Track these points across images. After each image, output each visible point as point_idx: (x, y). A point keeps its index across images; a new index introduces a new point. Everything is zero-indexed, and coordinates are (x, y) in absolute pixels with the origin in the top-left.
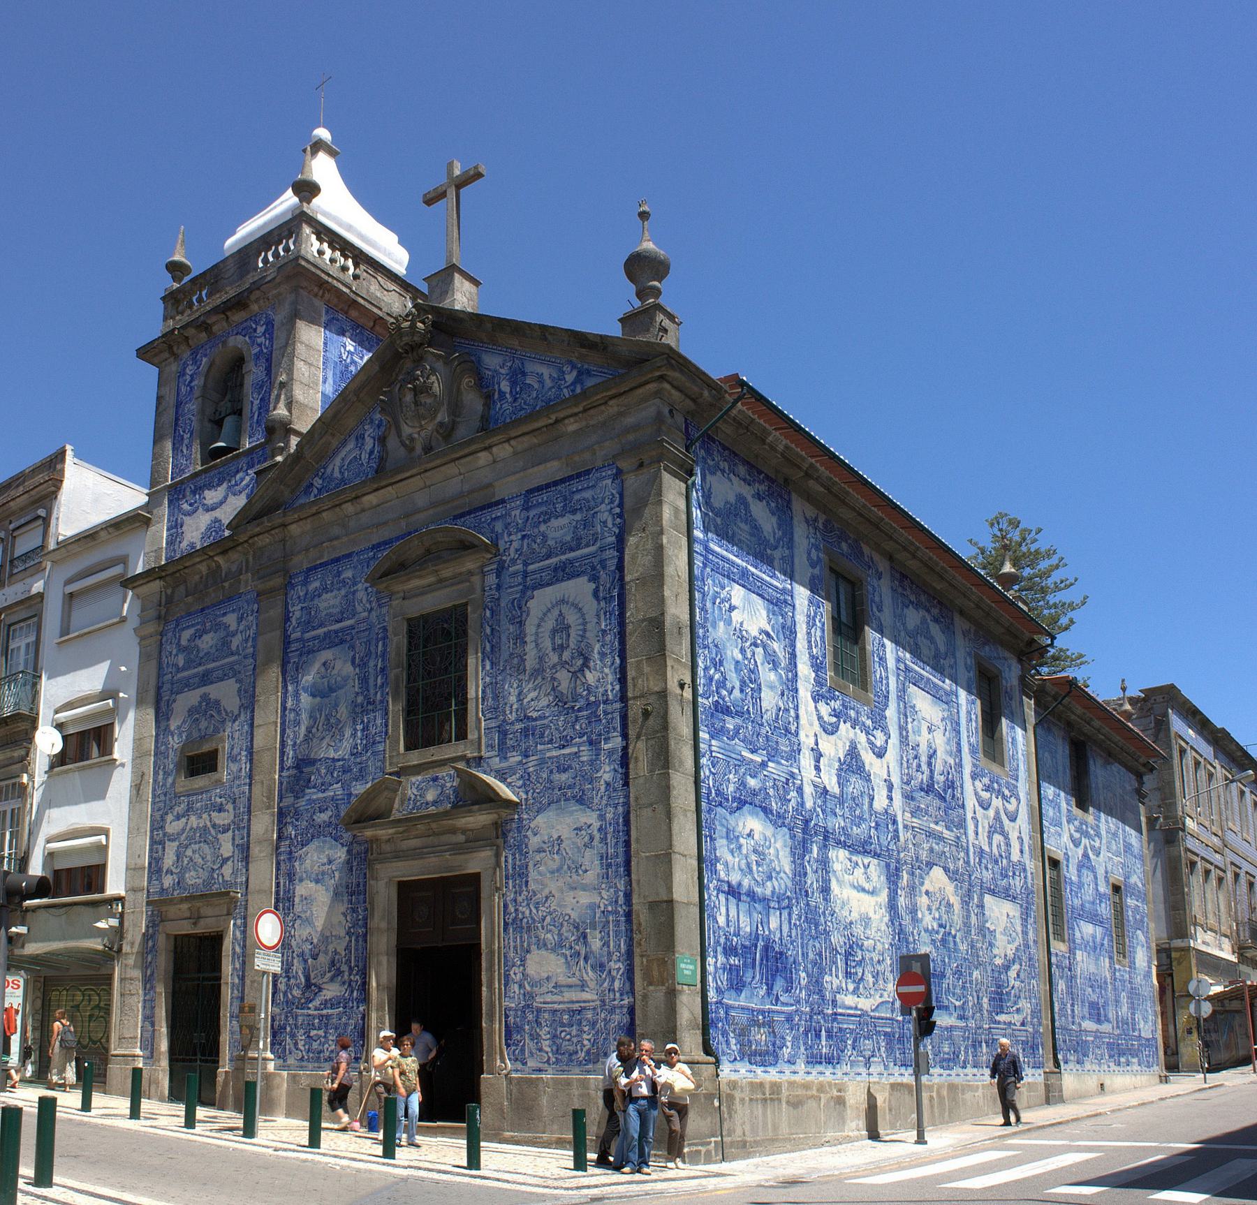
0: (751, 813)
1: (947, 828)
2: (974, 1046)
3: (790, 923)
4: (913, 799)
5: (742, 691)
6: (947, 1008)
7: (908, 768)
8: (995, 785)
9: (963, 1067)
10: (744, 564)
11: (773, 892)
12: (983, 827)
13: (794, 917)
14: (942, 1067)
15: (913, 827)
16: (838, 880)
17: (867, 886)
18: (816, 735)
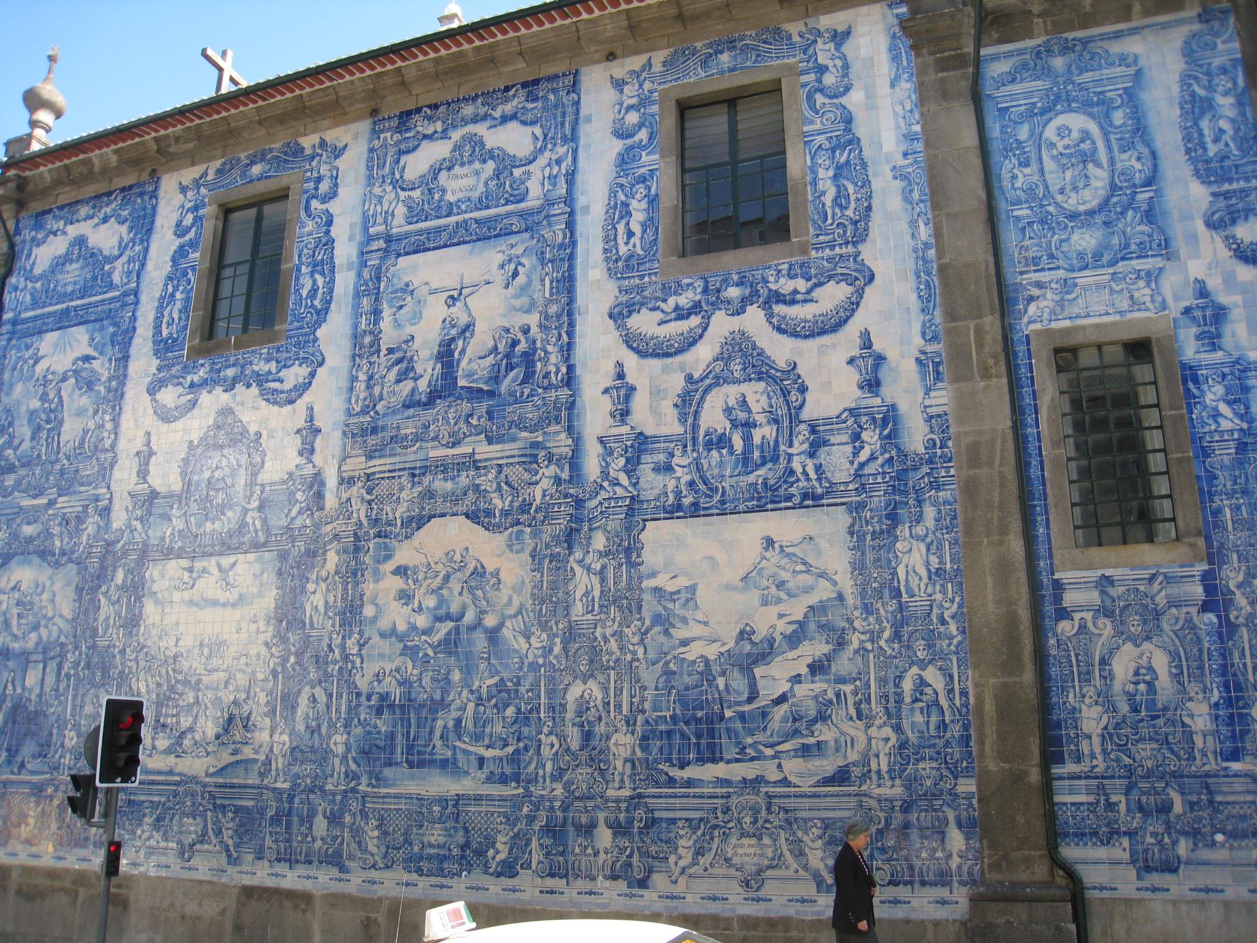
0: (21, 563)
1: (490, 441)
2: (554, 831)
3: (59, 674)
4: (374, 430)
5: (33, 439)
6: (444, 764)
7: (369, 387)
8: (733, 292)
9: (499, 875)
10: (65, 306)
11: (38, 644)
12: (657, 393)
13: (66, 666)
14: (420, 872)
15: (368, 477)
16: (157, 602)
17: (222, 596)
18: (148, 434)
